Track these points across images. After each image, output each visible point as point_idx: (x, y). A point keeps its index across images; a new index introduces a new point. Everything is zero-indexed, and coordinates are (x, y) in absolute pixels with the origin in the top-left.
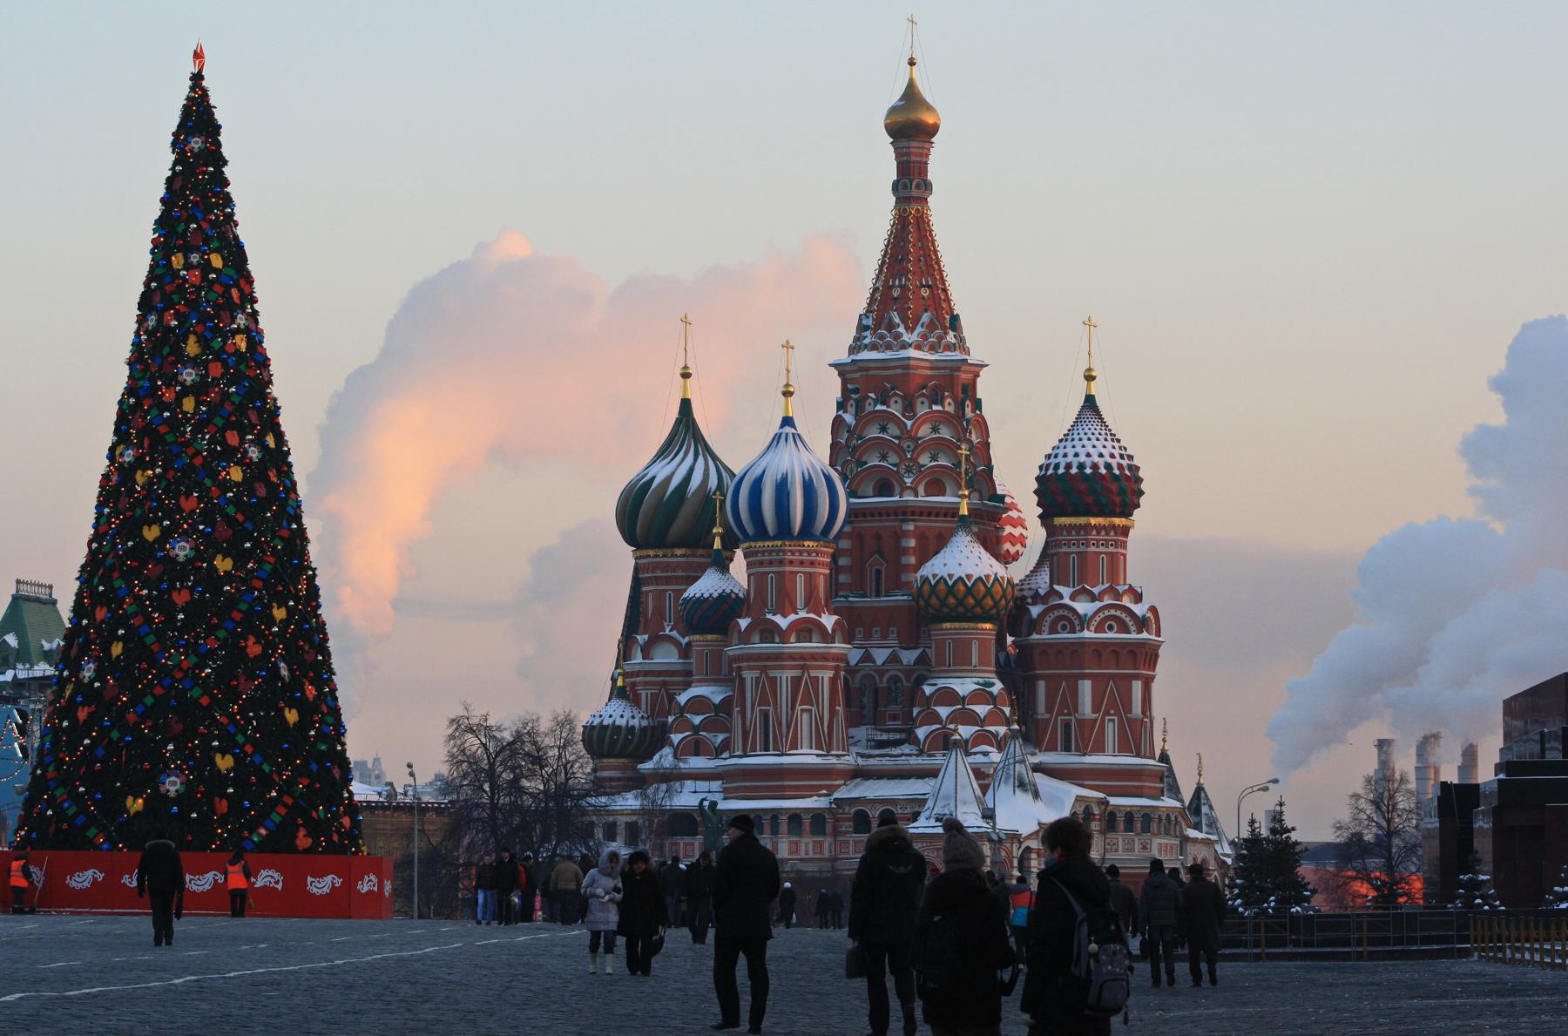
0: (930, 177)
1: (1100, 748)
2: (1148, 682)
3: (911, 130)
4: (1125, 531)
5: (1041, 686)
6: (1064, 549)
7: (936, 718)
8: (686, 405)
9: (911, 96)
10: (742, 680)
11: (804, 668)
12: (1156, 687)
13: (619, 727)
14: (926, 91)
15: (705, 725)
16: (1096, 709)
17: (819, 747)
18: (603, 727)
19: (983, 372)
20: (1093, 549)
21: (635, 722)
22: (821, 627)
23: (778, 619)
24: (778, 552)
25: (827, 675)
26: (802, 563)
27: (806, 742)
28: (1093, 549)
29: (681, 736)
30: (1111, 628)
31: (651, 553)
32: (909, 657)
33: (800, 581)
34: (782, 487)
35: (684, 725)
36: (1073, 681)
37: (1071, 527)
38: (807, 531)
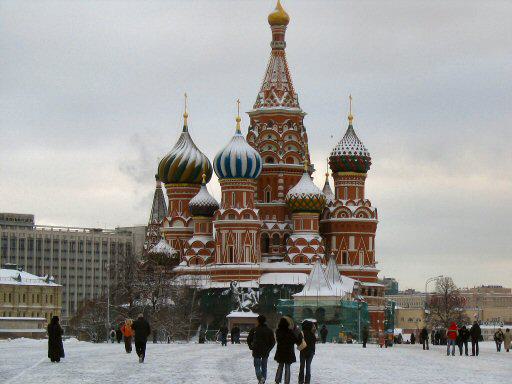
2: (374, 237)
5: (334, 238)
8: (185, 129)
11: (247, 230)
15: (200, 252)
17: (252, 261)
23: (236, 209)
25: (254, 232)
32: (282, 227)
33: (245, 195)
35: (191, 252)
37: (344, 177)
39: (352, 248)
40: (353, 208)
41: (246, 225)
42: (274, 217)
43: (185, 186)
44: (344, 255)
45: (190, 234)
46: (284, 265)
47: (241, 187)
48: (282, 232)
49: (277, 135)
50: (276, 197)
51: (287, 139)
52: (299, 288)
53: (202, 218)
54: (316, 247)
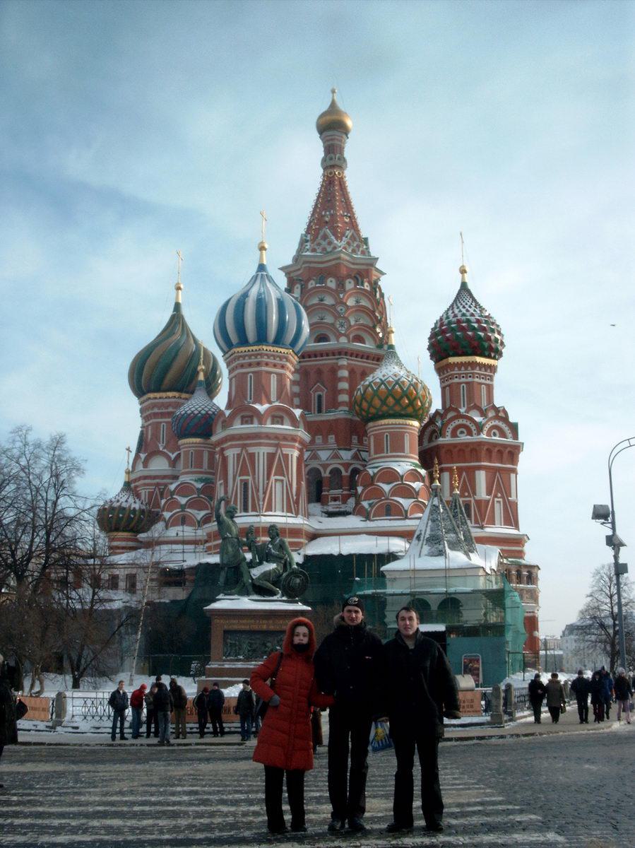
0: (347, 154)
4: (493, 369)
6: (456, 380)
7: (380, 492)
8: (177, 307)
9: (333, 107)
10: (225, 459)
13: (124, 509)
14: (341, 105)
15: (191, 504)
16: (489, 493)
17: (289, 510)
18: (112, 509)
19: (383, 278)
20: (476, 380)
21: (137, 506)
22: (292, 416)
23: (257, 406)
24: (256, 356)
26: (275, 366)
27: (279, 506)
28: (476, 380)
29: (170, 514)
30: (495, 435)
31: (151, 395)
32: (346, 455)
33: (274, 381)
34: (261, 304)
35: (172, 504)
36: (471, 472)
38: (278, 341)
41: (276, 437)
42: (332, 438)
44: (468, 506)
46: (353, 522)
47: (267, 364)
48: (346, 465)
49: (334, 293)
50: (334, 404)
52: (392, 557)
53: (198, 440)
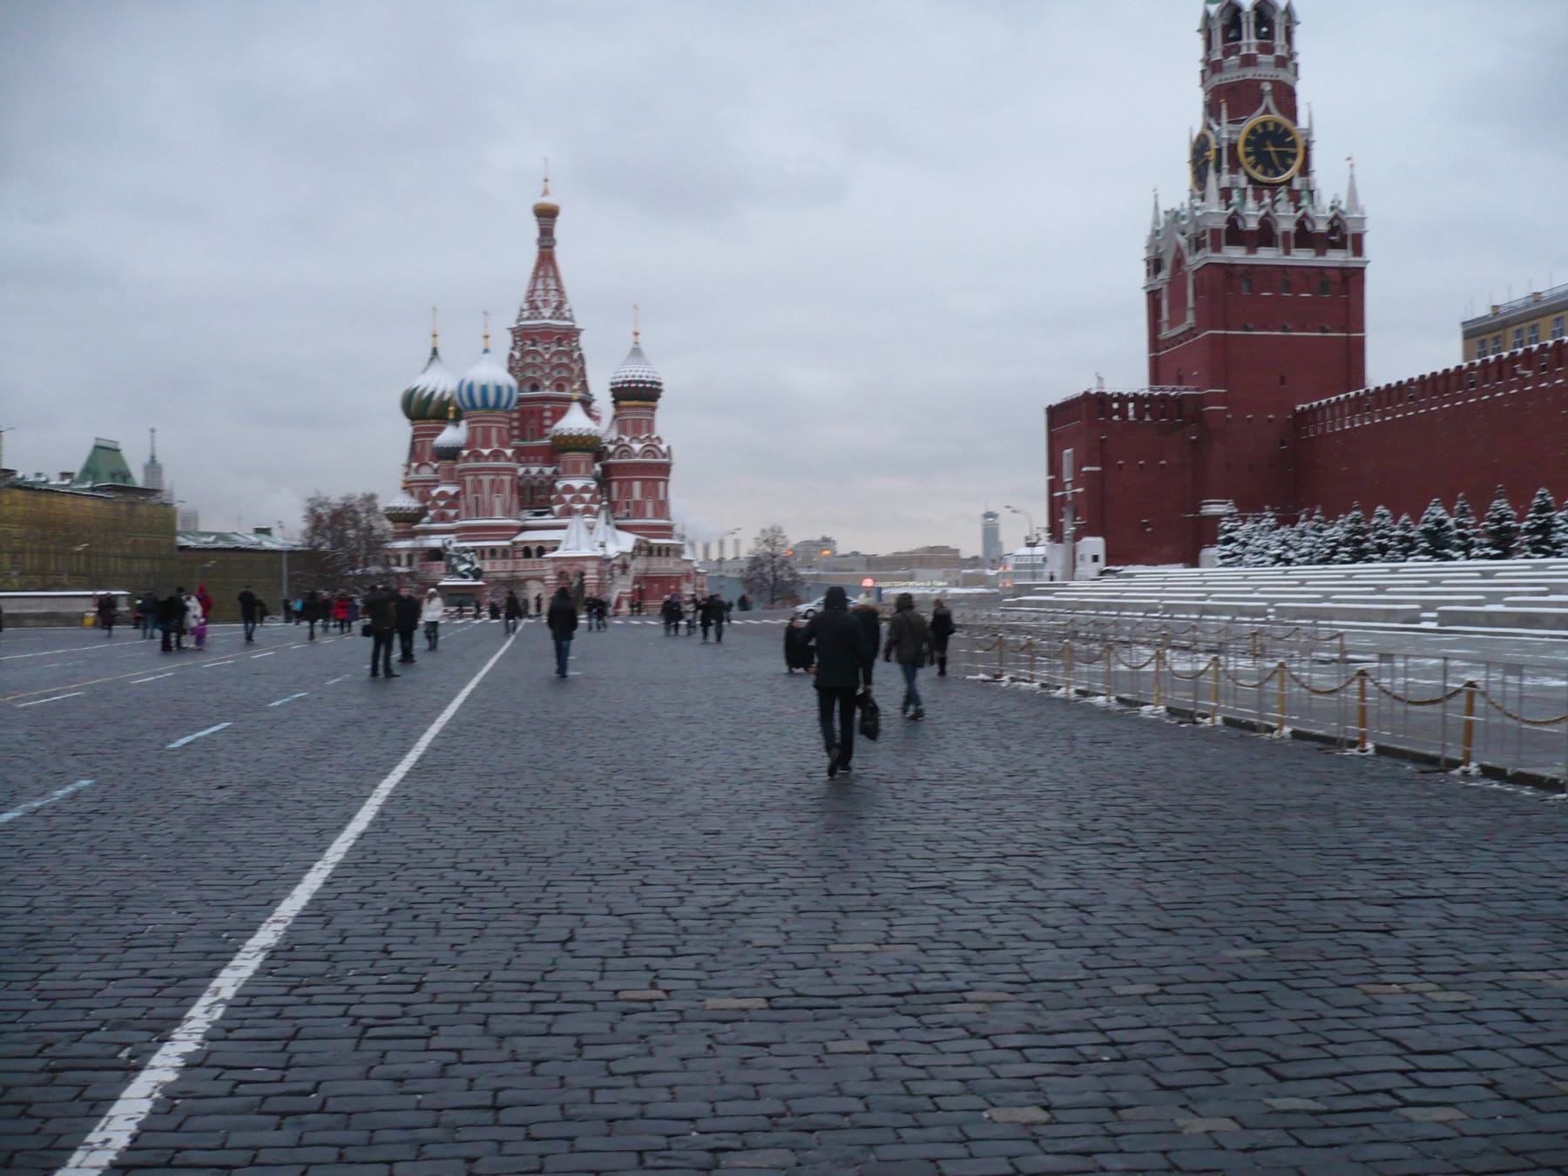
1: (643, 516)
2: (667, 481)
3: (546, 215)
4: (654, 408)
5: (615, 485)
12: (671, 484)
25: (507, 478)
32: (548, 471)
39: (637, 495)
40: (637, 447)
43: (432, 424)
45: (436, 483)
48: (549, 478)
50: (542, 436)
51: (555, 360)
54: (587, 496)
